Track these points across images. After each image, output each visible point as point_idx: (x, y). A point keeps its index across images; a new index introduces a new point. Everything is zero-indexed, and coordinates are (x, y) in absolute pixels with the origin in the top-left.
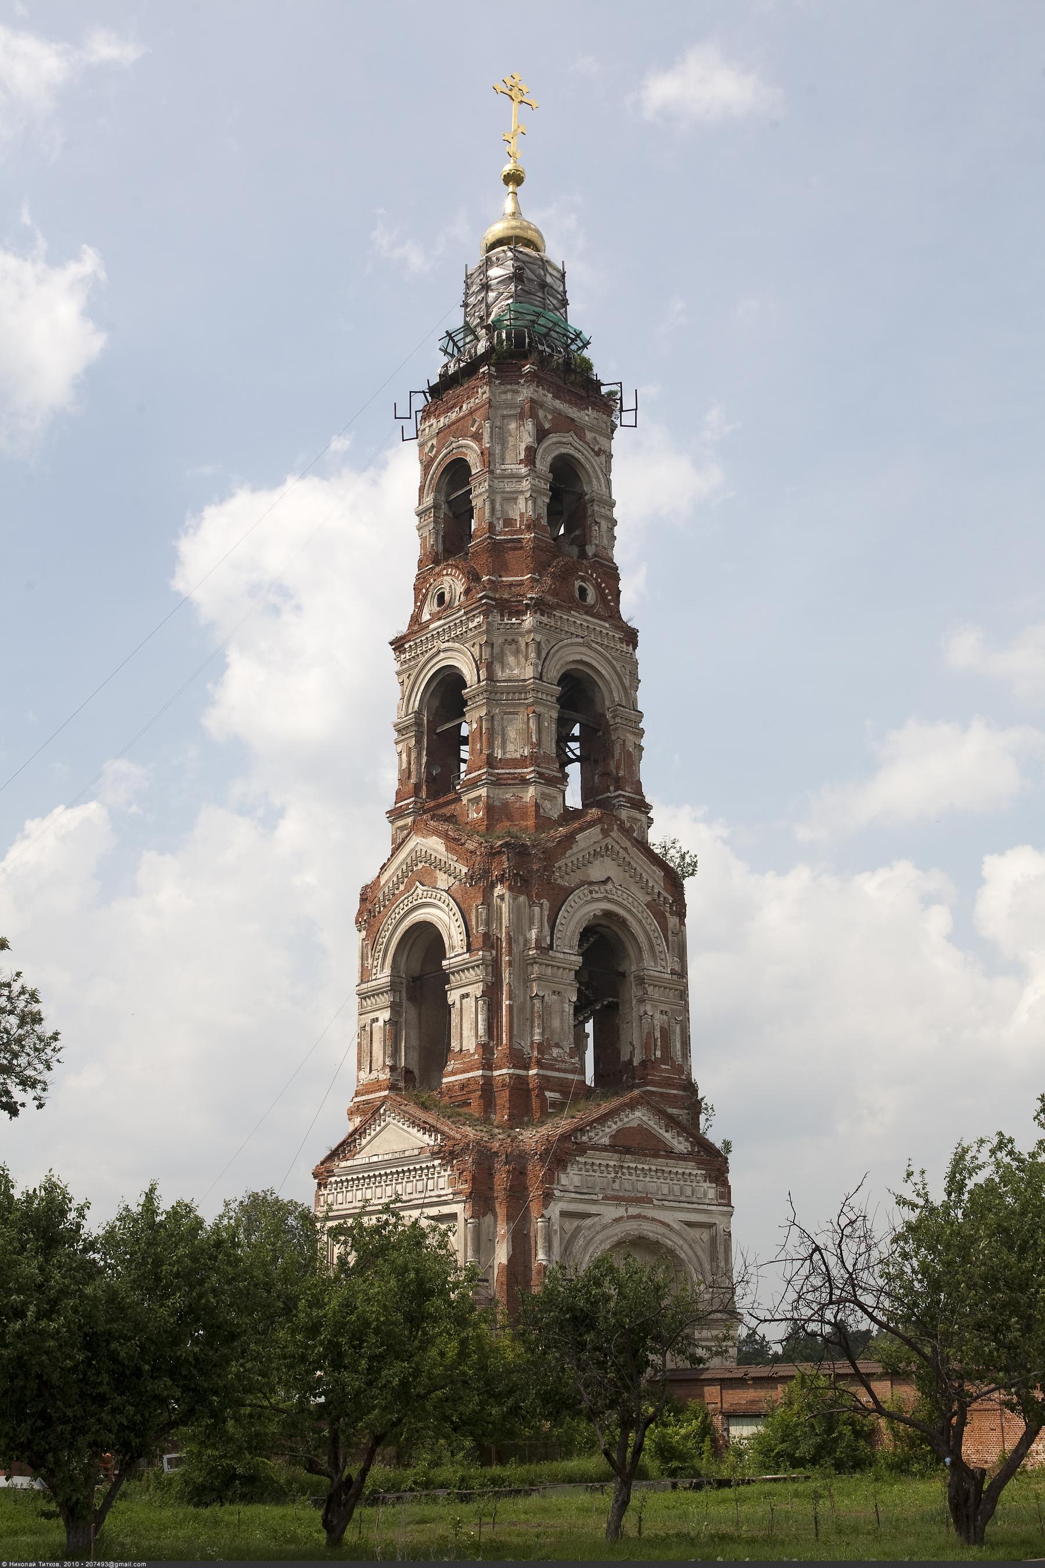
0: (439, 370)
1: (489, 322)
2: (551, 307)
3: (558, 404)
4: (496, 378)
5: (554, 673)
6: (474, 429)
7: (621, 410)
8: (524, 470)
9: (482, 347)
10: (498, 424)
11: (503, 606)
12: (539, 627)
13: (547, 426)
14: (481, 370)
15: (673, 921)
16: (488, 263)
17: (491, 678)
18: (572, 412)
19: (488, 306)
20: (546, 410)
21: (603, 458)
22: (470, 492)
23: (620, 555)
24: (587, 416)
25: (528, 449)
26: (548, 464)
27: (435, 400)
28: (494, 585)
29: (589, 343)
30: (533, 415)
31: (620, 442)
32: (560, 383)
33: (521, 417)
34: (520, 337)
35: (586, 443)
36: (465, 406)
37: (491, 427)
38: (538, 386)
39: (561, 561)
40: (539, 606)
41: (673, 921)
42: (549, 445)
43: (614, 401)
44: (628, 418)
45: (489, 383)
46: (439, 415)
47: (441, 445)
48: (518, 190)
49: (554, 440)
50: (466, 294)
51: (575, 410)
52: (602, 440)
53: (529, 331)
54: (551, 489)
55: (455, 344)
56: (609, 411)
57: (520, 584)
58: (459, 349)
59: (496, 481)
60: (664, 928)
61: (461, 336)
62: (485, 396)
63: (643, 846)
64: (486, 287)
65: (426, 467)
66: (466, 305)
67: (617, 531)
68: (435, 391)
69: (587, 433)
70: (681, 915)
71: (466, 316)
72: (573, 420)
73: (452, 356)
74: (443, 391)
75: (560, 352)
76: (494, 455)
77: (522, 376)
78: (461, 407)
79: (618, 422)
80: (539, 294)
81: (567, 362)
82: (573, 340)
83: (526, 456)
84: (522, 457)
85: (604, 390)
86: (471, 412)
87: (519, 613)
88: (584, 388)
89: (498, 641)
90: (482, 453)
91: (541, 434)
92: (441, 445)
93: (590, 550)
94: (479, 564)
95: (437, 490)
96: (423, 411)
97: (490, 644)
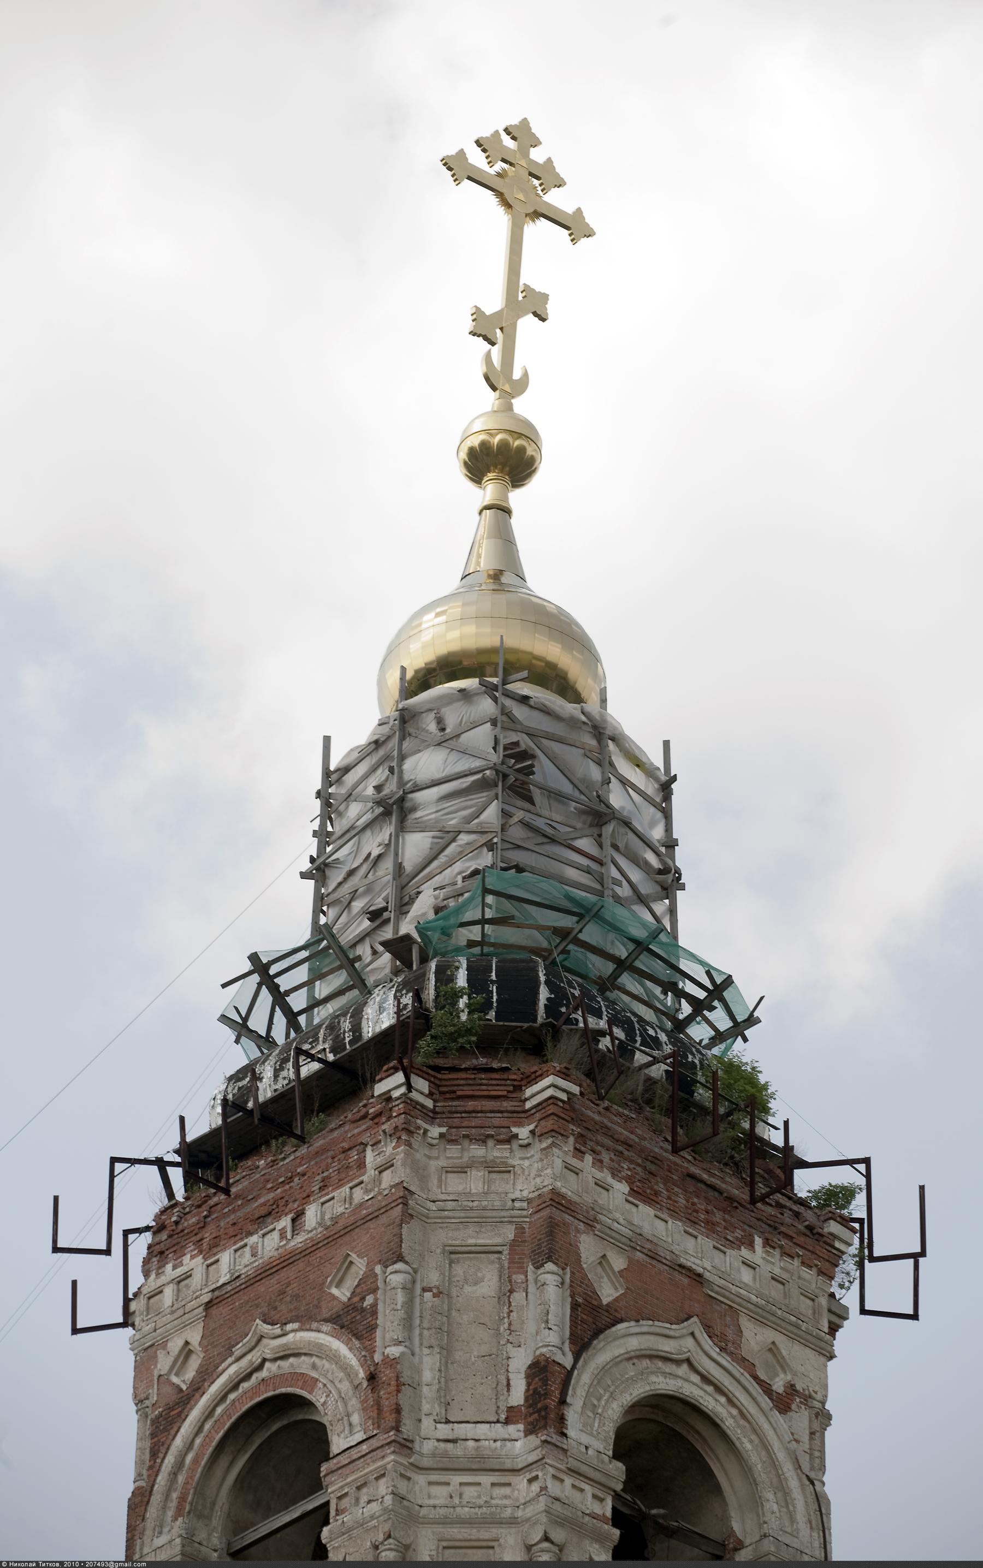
0: (216, 1086)
1: (407, 927)
2: (624, 891)
3: (645, 1218)
4: (433, 1116)
6: (342, 1293)
7: (867, 1255)
8: (520, 1445)
9: (379, 1016)
10: (433, 1278)
13: (608, 1293)
14: (380, 1088)
18: (697, 1250)
20: (607, 1236)
21: (801, 1419)
22: (322, 1515)
24: (747, 1269)
25: (540, 1370)
26: (610, 1429)
27: (202, 1191)
29: (752, 1020)
31: (864, 1373)
32: (659, 1147)
35: (742, 1361)
36: (312, 1214)
37: (409, 1289)
38: (579, 1153)
42: (616, 1362)
43: (846, 1221)
44: (887, 1285)
45: (405, 1132)
46: (215, 1245)
47: (219, 1348)
48: (517, 498)
49: (634, 1344)
50: (322, 836)
51: (706, 1243)
53: (551, 967)
54: (618, 1519)
55: (280, 999)
56: (825, 1258)
58: (292, 1017)
59: (421, 1480)
61: (301, 974)
62: (388, 1178)
65: (160, 1424)
68: (204, 1160)
69: (748, 1328)
71: (318, 910)
72: (697, 1278)
73: (266, 1041)
74: (228, 1158)
75: (656, 1043)
76: (416, 1386)
77: (521, 1115)
78: (298, 1218)
79: (850, 1299)
80: (584, 843)
81: (682, 1078)
82: (699, 1007)
83: (533, 1396)
84: (518, 1396)
85: (805, 1183)
88: (737, 1168)
90: (372, 1378)
91: (590, 1322)
92: (219, 1348)
95: (195, 1507)
96: (158, 1229)
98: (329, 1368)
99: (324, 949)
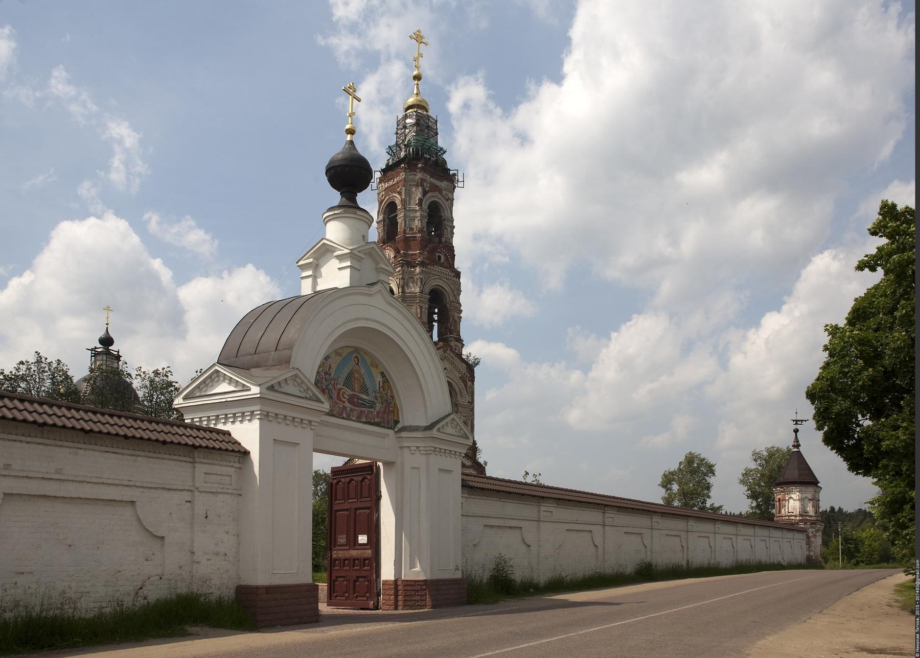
3: (432, 180)
5: (427, 290)
9: (403, 154)
11: (408, 264)
12: (422, 272)
15: (469, 383)
16: (406, 117)
17: (403, 292)
18: (438, 183)
19: (406, 136)
23: (456, 242)
24: (443, 184)
28: (405, 255)
30: (422, 185)
33: (417, 186)
34: (417, 151)
39: (431, 245)
40: (422, 264)
41: (469, 383)
44: (460, 184)
47: (386, 195)
52: (450, 194)
57: (415, 254)
60: (466, 387)
63: (459, 355)
64: (405, 127)
65: (380, 203)
66: (397, 133)
67: (455, 230)
70: (473, 381)
81: (436, 162)
86: (398, 183)
87: (414, 267)
89: (406, 277)
91: (425, 193)
92: (386, 195)
93: (443, 240)
94: (400, 245)
95: (384, 214)
97: (403, 278)
98: (398, 200)
99: (397, 145)
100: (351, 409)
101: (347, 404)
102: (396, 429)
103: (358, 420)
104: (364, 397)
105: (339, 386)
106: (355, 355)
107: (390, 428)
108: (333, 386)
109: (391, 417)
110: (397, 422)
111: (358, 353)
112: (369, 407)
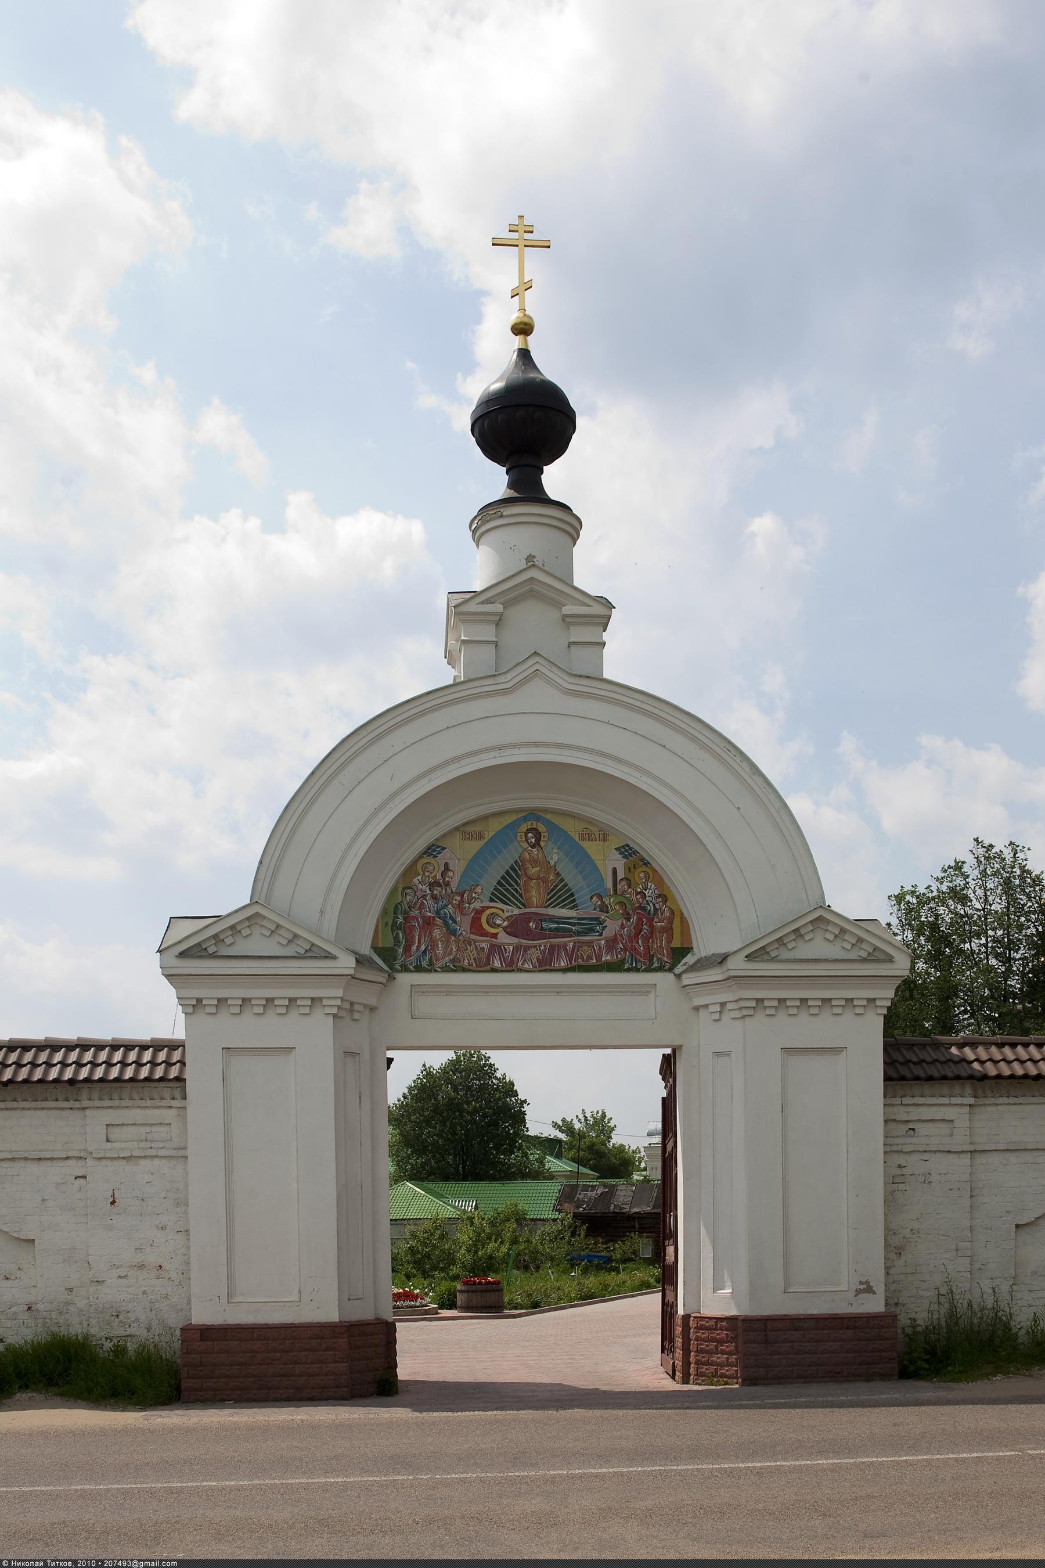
100: (517, 948)
101: (503, 938)
102: (679, 969)
103: (545, 965)
104: (564, 912)
105: (477, 905)
106: (524, 827)
107: (660, 969)
108: (460, 906)
109: (660, 943)
110: (685, 950)
111: (538, 819)
112: (579, 934)
